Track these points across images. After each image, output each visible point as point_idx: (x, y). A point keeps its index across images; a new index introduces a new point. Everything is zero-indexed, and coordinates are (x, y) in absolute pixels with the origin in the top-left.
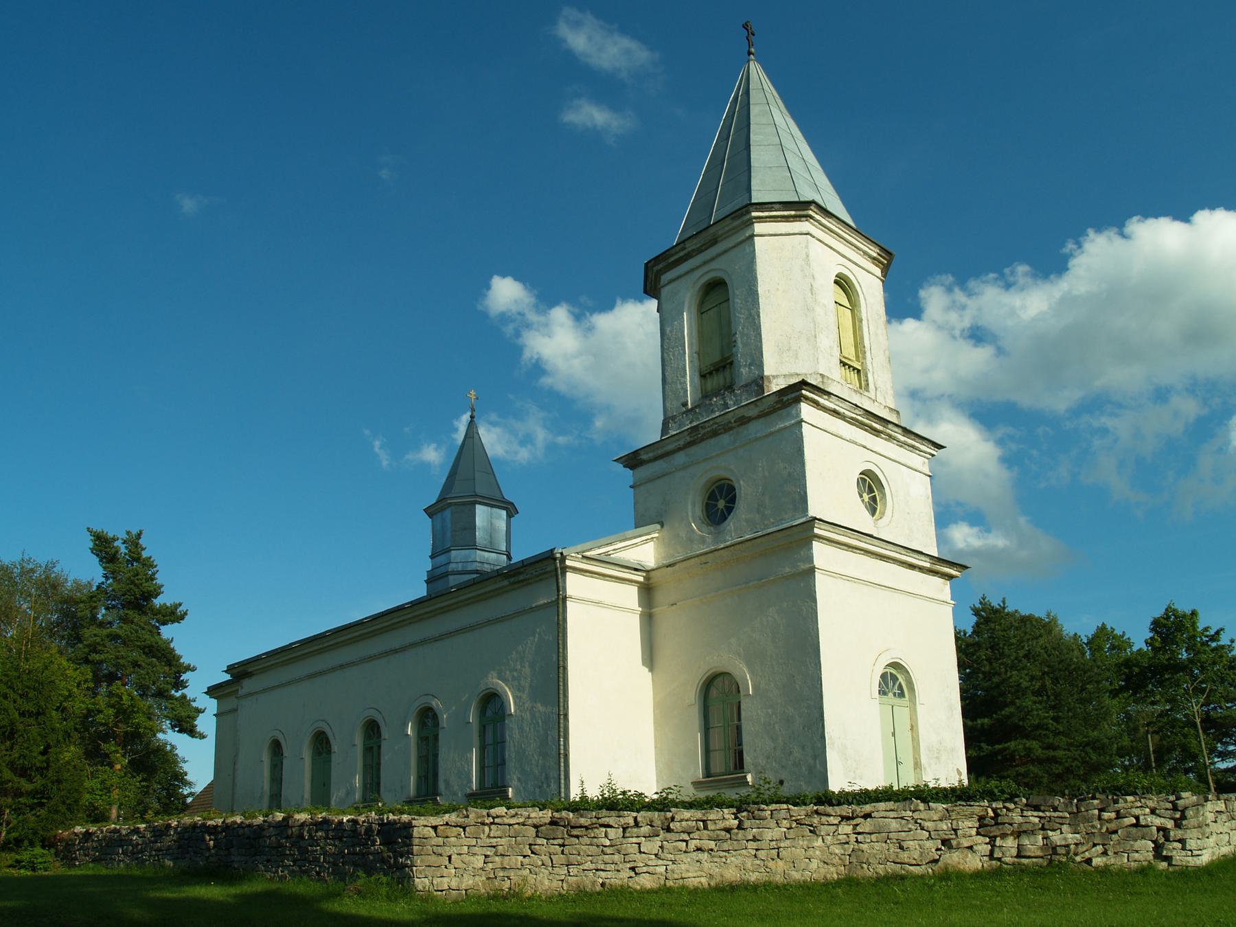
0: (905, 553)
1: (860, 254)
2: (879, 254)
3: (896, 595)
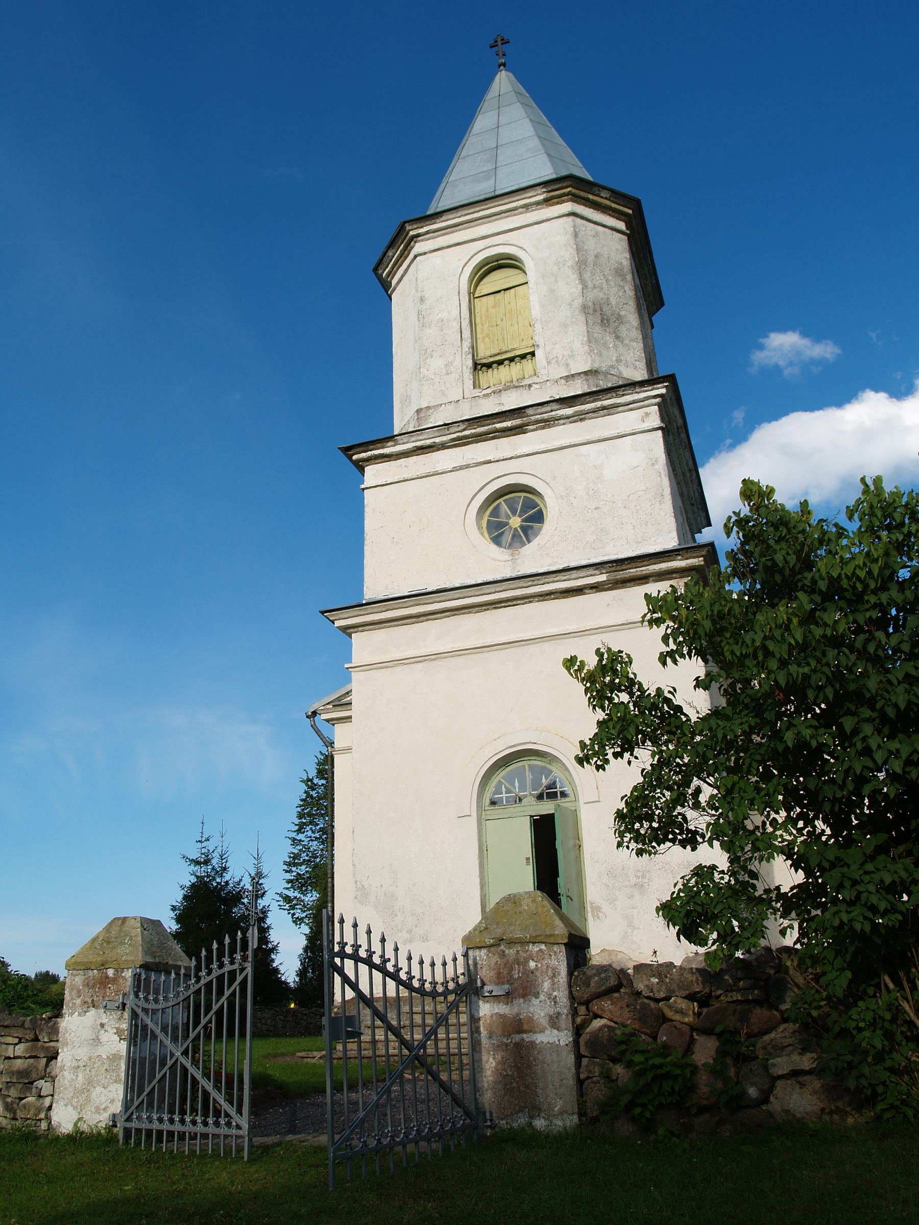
0: (530, 583)
1: (522, 213)
2: (549, 192)
3: (533, 648)
